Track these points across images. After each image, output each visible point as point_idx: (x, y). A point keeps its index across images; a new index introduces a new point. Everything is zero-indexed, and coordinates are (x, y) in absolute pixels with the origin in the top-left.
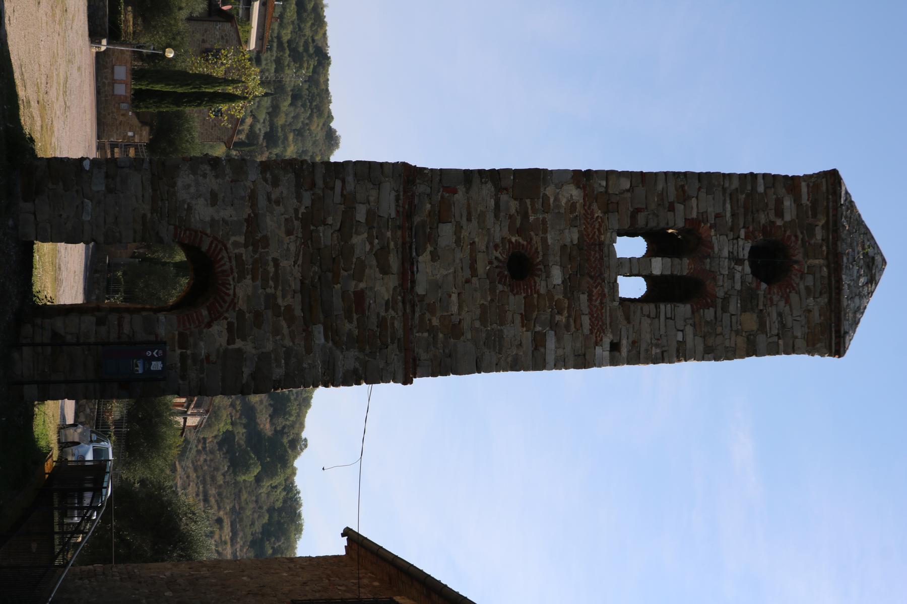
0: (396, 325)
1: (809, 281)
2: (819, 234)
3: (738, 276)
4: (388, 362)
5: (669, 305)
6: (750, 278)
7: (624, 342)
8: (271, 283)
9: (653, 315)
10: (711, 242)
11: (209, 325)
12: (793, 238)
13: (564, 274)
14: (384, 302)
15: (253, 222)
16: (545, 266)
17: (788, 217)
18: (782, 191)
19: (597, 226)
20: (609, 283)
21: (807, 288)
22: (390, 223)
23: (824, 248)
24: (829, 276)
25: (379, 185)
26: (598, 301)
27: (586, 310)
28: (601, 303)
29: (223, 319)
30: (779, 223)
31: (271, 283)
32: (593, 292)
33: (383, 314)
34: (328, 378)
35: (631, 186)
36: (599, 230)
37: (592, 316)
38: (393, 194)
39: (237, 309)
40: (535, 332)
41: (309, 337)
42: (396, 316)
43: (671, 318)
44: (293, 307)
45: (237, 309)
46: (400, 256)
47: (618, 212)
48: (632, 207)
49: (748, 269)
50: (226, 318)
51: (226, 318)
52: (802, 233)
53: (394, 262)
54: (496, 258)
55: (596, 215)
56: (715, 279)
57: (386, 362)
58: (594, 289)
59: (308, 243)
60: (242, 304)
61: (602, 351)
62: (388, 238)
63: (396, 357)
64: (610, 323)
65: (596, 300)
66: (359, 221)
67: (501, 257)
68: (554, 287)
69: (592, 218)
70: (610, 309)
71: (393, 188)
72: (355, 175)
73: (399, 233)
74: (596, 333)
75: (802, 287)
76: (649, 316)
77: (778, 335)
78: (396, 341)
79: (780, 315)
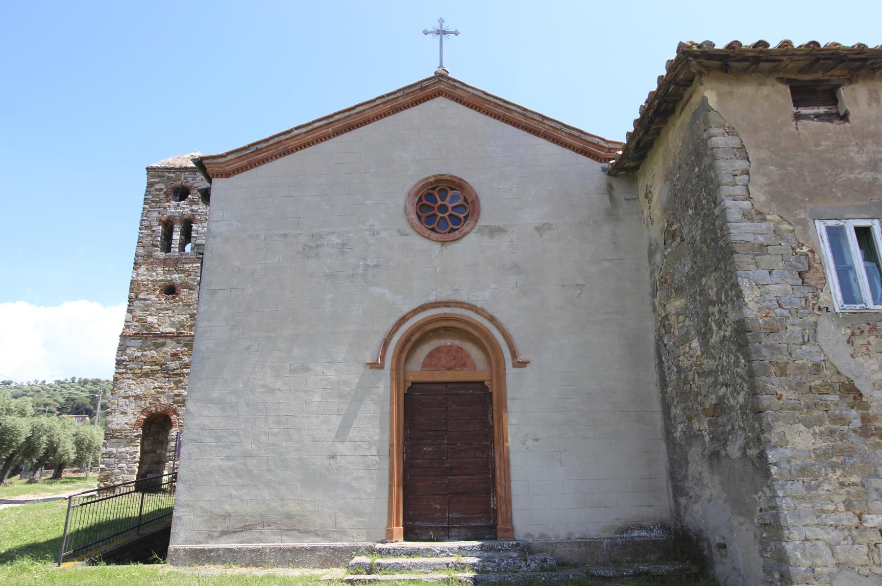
8: (163, 390)
11: (178, 415)
13: (175, 273)
15: (137, 397)
17: (163, 187)
18: (153, 189)
30: (165, 190)
31: (163, 390)
33: (182, 345)
73: (149, 338)
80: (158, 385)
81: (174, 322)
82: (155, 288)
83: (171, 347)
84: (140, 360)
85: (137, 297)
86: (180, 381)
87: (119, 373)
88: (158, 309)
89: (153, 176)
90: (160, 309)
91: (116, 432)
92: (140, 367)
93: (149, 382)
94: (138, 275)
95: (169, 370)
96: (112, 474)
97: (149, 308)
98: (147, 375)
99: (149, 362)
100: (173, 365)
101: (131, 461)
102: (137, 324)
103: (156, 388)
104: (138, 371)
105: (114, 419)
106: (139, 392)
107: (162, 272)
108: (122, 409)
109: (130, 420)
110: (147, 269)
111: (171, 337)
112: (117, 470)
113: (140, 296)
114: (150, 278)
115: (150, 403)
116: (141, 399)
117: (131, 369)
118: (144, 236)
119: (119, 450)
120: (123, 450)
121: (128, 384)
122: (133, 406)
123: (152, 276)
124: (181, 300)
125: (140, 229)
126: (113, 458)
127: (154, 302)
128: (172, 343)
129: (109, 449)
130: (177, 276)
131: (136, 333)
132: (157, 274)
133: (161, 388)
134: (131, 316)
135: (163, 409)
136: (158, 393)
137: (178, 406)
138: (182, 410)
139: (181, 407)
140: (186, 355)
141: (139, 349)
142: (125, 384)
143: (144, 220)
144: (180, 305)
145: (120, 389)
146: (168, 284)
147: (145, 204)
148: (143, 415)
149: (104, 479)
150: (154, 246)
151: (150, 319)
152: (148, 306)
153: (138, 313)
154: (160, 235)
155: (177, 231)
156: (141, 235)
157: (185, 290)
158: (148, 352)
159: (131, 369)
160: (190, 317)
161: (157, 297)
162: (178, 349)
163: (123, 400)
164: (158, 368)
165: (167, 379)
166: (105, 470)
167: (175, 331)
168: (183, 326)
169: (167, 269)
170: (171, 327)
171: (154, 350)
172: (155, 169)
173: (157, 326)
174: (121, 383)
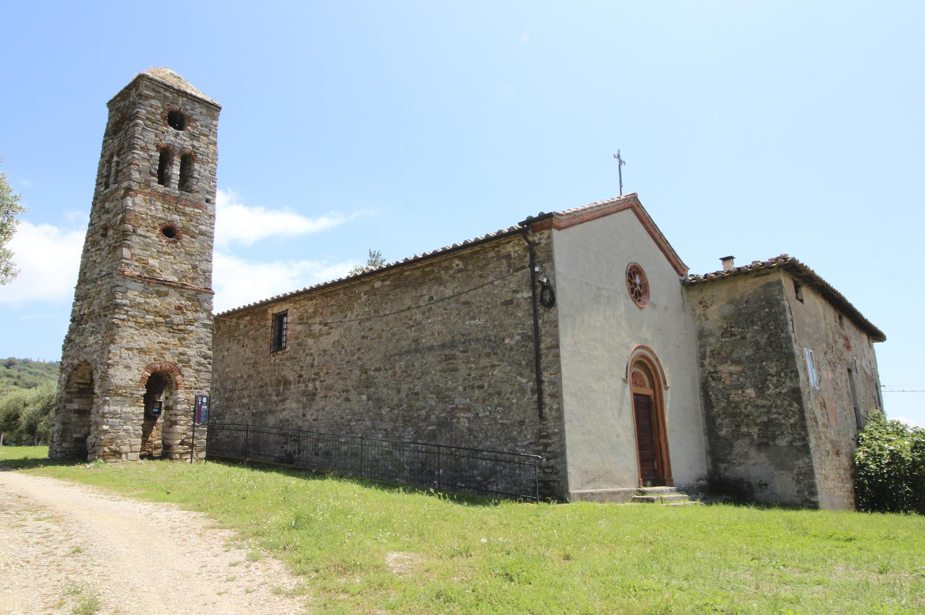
2: (168, 94)
8: (168, 346)
10: (168, 144)
11: (183, 376)
13: (175, 214)
15: (141, 351)
23: (175, 95)
31: (168, 346)
38: (133, 283)
41: (191, 332)
53: (164, 289)
56: (184, 148)
73: (151, 284)
80: (163, 340)
81: (176, 270)
83: (174, 299)
84: (142, 307)
86: (184, 339)
88: (158, 252)
90: (162, 252)
93: (153, 334)
95: (174, 324)
98: (150, 326)
100: (177, 319)
103: (160, 343)
104: (140, 320)
106: (143, 345)
108: (125, 362)
109: (135, 376)
111: (174, 287)
115: (155, 360)
117: (133, 317)
120: (128, 410)
122: (137, 359)
124: (183, 246)
130: (178, 218)
132: (156, 209)
133: (166, 344)
135: (168, 367)
136: (163, 348)
137: (183, 366)
138: (188, 371)
139: (186, 367)
140: (190, 310)
141: (140, 294)
142: (127, 333)
148: (148, 371)
151: (151, 261)
155: (177, 165)
159: (133, 317)
161: (157, 237)
162: (183, 302)
163: (126, 351)
168: (185, 277)
169: (166, 206)
174: (123, 331)
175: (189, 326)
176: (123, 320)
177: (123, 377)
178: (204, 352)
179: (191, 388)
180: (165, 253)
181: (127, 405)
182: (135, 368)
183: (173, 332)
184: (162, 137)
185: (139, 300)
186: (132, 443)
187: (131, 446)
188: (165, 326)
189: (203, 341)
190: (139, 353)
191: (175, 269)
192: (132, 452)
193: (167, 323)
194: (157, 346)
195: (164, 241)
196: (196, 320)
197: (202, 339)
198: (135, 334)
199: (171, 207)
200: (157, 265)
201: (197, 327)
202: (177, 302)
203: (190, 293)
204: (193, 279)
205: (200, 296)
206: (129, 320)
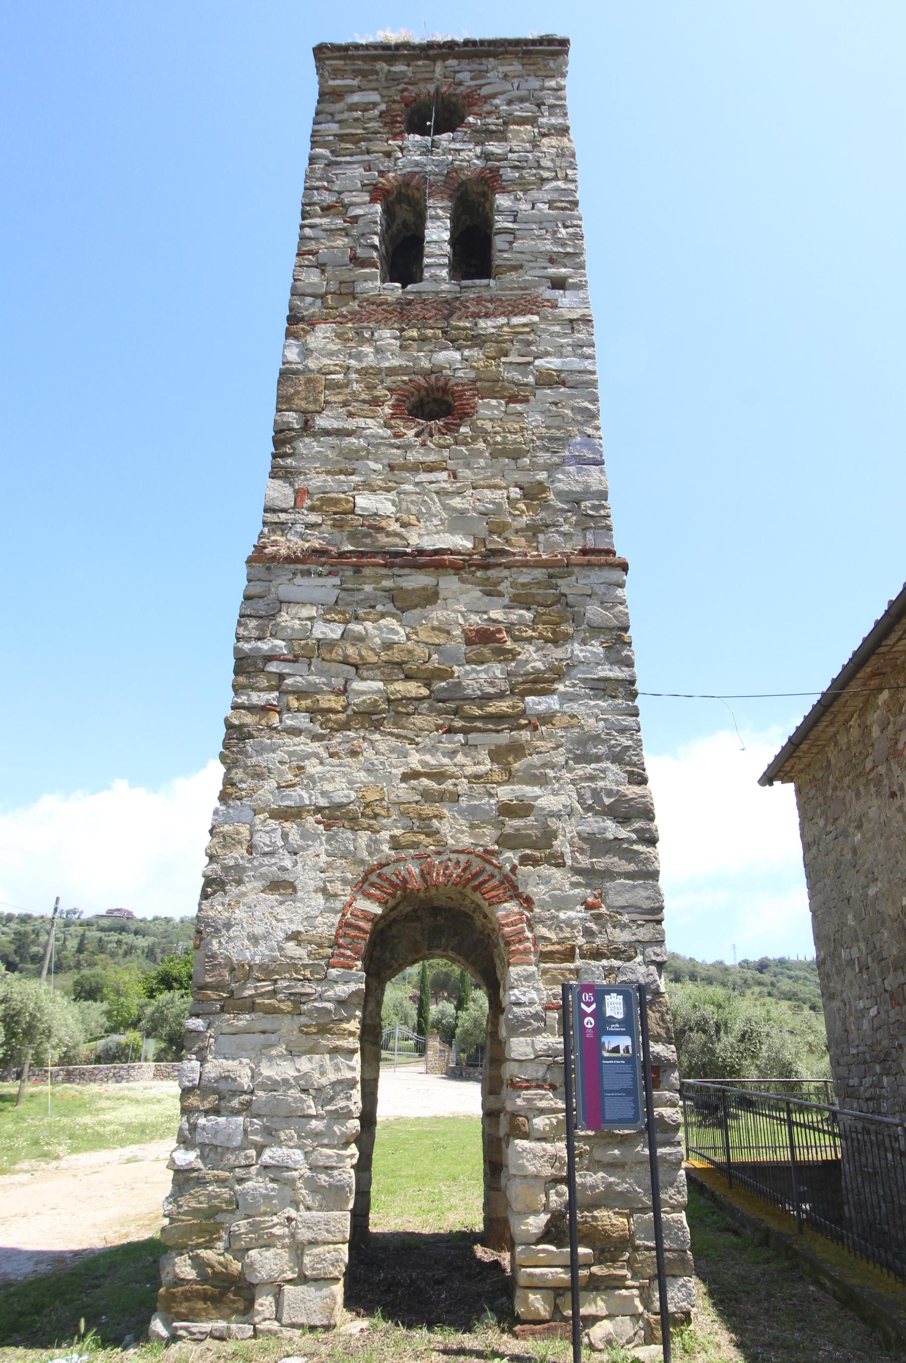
0: (526, 581)
1: (465, 76)
2: (399, 68)
3: (458, 146)
4: (589, 592)
5: (496, 217)
6: (459, 134)
7: (552, 271)
8: (448, 785)
9: (510, 238)
10: (405, 175)
11: (528, 902)
12: (406, 94)
13: (446, 348)
14: (487, 599)
16: (432, 372)
18: (340, 106)
19: (372, 307)
20: (461, 293)
21: (472, 79)
22: (350, 586)
23: (420, 63)
24: (458, 57)
25: (281, 602)
26: (489, 305)
27: (502, 320)
28: (491, 301)
29: (515, 875)
30: (383, 107)
31: (448, 785)
32: (473, 313)
33: (506, 601)
34: (620, 689)
35: (317, 267)
36: (379, 305)
37: (511, 312)
38: (299, 580)
39: (496, 847)
40: (536, 384)
41: (547, 718)
42: (510, 579)
43: (515, 216)
44: (493, 748)
45: (496, 847)
46: (407, 571)
47: (353, 282)
48: (347, 265)
49: (445, 136)
50: (514, 869)
51: (514, 869)
52: (398, 85)
54: (417, 435)
55: (357, 308)
57: (589, 596)
58: (470, 310)
59: (377, 720)
60: (488, 837)
61: (566, 300)
62: (375, 589)
63: (581, 581)
64: (522, 289)
65: (486, 307)
66: (343, 634)
67: (416, 430)
68: (467, 360)
69: (358, 313)
70: (503, 290)
71: (290, 580)
72: (259, 639)
73: (367, 571)
74: (538, 307)
75: (472, 83)
76: (511, 243)
77: (538, 106)
78: (554, 581)
79: (510, 103)
80: (424, 763)
81: (463, 512)
82: (378, 394)
84: (337, 654)
85: (307, 427)
86: (517, 750)
87: (251, 709)
88: (392, 468)
89: (336, 73)
90: (404, 468)
91: (248, 977)
92: (338, 683)
93: (382, 747)
94: (306, 352)
96: (235, 1204)
97: (357, 465)
99: (374, 666)
101: (328, 1132)
102: (314, 518)
103: (415, 775)
105: (239, 914)
107: (398, 343)
108: (269, 866)
110: (339, 336)
111: (457, 568)
112: (257, 1185)
113: (322, 422)
114: (353, 362)
115: (395, 843)
116: (354, 822)
117: (300, 694)
118: (321, 234)
119: (267, 1071)
120: (285, 1070)
121: (291, 754)
123: (359, 357)
124: (480, 433)
125: (305, 215)
126: (236, 1112)
127: (375, 444)
128: (466, 592)
129: (215, 1067)
130: (457, 355)
131: (315, 551)
132: (378, 351)
133: (439, 776)
134: (289, 491)
136: (427, 795)
137: (524, 860)
138: (547, 881)
139: (536, 862)
140: (529, 640)
141: (329, 610)
142: (279, 755)
143: (317, 188)
144: (479, 454)
145: (259, 776)
146: (422, 381)
147: (314, 144)
148: (369, 896)
149: (190, 1231)
150: (357, 261)
151: (364, 501)
152: (354, 455)
153: (316, 481)
154: (378, 229)
156: (308, 231)
157: (494, 402)
158: (368, 624)
160: (525, 496)
161: (386, 425)
164: (413, 688)
165: (460, 737)
166: (201, 1182)
167: (470, 545)
169: (415, 333)
170: (452, 530)
171: (393, 616)
172: (345, 48)
173: (395, 527)
174: (261, 750)
175: (529, 699)
176: (266, 709)
177: (259, 930)
178: (610, 793)
179: (569, 955)
180: (416, 468)
181: (282, 1049)
182: (312, 885)
183: (465, 731)
184: (387, 163)
185: (321, 630)
186: (304, 1235)
187: (298, 1249)
188: (431, 709)
189: (602, 749)
190: (328, 827)
191: (454, 509)
192: (303, 1279)
193: (436, 698)
194: (403, 791)
195: (411, 433)
196: (559, 673)
197: (596, 739)
198: (308, 756)
199: (429, 332)
200: (389, 509)
201: (567, 698)
202: (474, 618)
203: (523, 579)
204: (533, 531)
205: (564, 586)
206: (289, 710)
